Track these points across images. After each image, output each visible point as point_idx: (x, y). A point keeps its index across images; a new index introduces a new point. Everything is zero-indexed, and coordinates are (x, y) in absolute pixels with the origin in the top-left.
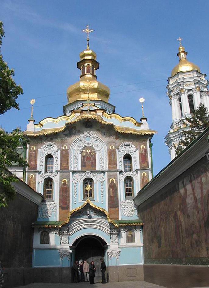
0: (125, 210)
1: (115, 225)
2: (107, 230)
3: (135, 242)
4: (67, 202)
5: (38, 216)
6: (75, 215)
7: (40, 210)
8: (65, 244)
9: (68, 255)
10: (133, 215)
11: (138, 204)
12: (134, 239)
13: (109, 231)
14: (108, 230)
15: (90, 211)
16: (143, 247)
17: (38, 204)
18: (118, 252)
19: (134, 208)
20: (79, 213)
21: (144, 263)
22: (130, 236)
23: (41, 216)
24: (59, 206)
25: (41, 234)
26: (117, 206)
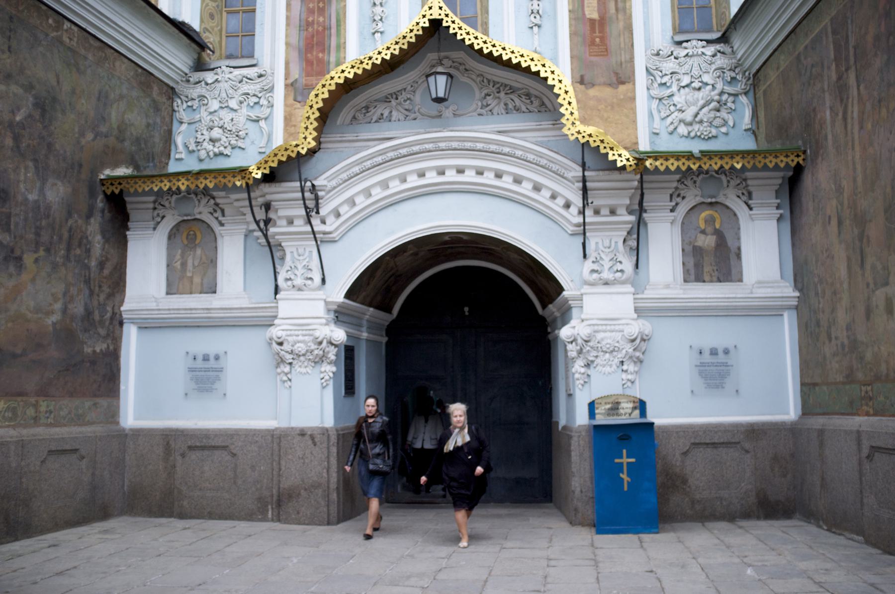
0: (676, 99)
1: (611, 158)
2: (560, 201)
3: (741, 280)
4: (333, 59)
5: (173, 147)
6: (360, 116)
7: (182, 113)
8: (300, 289)
9: (320, 360)
10: (724, 130)
11: (754, 60)
12: (733, 261)
13: (574, 210)
14: (567, 206)
15: (450, 76)
16: (794, 313)
17: (171, 84)
18: (633, 341)
19: (728, 89)
20: (386, 100)
21: (800, 412)
22: (708, 241)
23: (187, 147)
24: (286, 86)
25: (171, 237)
26: (622, 77)
